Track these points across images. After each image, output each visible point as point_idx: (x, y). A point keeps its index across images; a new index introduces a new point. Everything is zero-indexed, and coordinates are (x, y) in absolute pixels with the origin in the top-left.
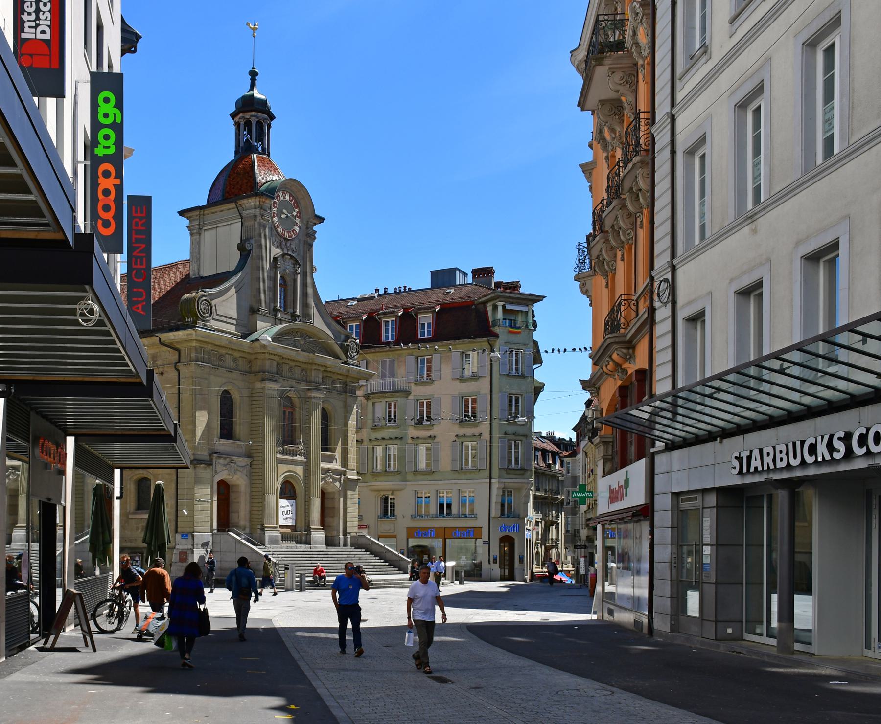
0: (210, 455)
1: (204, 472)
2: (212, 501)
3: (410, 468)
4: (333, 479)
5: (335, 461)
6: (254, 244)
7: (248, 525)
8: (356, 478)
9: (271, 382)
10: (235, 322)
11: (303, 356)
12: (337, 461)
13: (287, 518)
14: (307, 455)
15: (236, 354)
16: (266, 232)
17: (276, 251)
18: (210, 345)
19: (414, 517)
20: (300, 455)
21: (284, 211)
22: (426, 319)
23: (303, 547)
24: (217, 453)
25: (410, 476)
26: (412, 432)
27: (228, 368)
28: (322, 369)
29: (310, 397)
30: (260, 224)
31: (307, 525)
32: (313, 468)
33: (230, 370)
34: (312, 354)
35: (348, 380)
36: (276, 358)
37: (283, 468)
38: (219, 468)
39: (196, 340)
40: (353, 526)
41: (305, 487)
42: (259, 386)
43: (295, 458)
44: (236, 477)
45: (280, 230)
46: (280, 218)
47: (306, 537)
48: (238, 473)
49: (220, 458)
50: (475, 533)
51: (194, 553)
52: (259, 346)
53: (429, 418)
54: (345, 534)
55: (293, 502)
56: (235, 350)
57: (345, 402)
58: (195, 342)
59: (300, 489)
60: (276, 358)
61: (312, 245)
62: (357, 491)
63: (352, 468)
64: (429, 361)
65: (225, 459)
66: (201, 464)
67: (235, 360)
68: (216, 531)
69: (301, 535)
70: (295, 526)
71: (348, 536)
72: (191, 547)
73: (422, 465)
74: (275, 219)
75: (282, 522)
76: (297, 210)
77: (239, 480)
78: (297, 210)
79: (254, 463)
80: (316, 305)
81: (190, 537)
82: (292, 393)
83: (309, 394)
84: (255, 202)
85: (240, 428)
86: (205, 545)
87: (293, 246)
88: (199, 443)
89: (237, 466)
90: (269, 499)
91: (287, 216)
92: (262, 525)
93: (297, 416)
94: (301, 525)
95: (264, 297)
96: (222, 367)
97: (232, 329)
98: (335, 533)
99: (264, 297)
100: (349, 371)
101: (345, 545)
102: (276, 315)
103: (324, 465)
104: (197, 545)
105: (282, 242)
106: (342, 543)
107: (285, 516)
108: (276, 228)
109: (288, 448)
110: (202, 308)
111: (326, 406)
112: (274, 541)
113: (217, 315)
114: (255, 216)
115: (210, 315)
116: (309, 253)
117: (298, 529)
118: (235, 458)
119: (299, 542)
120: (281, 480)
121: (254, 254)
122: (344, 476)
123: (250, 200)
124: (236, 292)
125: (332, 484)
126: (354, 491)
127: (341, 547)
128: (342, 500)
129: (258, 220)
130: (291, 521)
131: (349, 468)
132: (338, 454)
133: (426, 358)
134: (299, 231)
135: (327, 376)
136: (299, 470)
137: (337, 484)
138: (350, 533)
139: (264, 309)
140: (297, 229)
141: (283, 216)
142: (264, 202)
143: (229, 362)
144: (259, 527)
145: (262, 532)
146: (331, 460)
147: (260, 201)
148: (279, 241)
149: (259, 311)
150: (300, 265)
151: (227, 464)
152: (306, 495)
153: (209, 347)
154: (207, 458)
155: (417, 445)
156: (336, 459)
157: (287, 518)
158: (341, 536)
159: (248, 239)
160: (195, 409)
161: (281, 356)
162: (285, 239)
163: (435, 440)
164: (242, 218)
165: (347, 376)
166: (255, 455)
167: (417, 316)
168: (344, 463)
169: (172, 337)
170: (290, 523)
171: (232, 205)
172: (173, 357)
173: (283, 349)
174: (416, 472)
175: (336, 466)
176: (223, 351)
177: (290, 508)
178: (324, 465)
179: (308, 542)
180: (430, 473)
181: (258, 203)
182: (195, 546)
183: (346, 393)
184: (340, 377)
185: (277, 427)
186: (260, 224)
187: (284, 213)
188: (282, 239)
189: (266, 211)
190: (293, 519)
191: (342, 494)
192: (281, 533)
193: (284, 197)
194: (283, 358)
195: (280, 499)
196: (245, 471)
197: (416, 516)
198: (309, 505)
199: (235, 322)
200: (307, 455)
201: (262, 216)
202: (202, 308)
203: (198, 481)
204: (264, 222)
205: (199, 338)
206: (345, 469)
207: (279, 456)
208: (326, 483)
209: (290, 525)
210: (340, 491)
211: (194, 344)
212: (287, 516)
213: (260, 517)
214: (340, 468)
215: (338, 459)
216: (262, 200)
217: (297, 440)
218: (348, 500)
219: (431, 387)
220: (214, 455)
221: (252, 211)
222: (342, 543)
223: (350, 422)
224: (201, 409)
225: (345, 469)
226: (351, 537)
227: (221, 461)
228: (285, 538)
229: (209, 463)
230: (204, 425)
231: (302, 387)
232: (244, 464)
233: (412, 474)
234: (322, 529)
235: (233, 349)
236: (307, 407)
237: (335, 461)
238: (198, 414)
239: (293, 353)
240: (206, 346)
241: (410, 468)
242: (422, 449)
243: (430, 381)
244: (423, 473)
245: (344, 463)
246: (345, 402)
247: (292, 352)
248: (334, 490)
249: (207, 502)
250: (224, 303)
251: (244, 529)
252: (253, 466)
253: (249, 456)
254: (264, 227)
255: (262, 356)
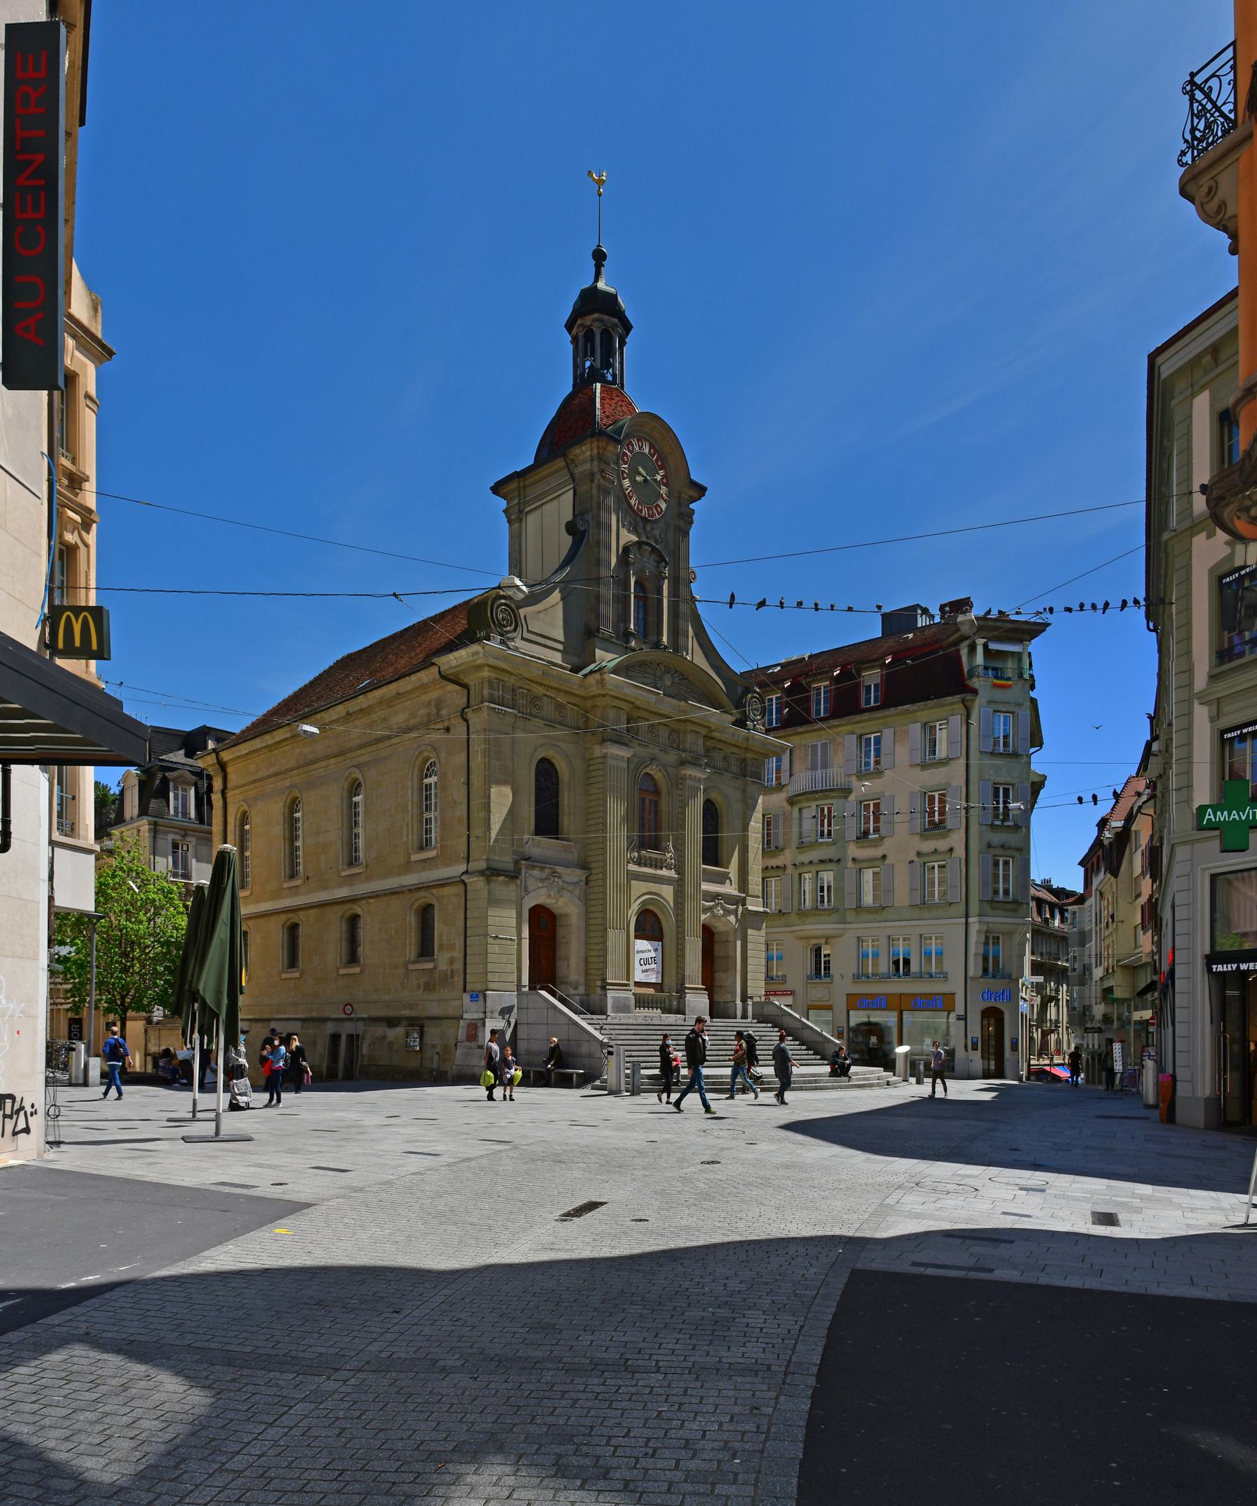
0: (517, 863)
1: (501, 887)
2: (520, 939)
3: (850, 902)
4: (724, 909)
5: (728, 881)
6: (590, 521)
7: (582, 980)
8: (761, 909)
9: (617, 745)
10: (560, 647)
11: (669, 706)
12: (731, 881)
13: (647, 971)
14: (680, 869)
15: (561, 699)
16: (611, 501)
17: (628, 537)
18: (513, 677)
19: (857, 977)
20: (667, 868)
21: (640, 469)
22: (872, 677)
23: (672, 1018)
24: (527, 859)
25: (850, 916)
26: (853, 851)
27: (547, 720)
28: (703, 731)
29: (684, 778)
30: (599, 486)
31: (680, 982)
32: (688, 889)
33: (551, 724)
34: (683, 703)
35: (749, 756)
36: (625, 706)
37: (638, 887)
38: (531, 884)
39: (489, 666)
40: (757, 988)
41: (677, 921)
42: (598, 751)
43: (659, 872)
44: (562, 901)
45: (633, 502)
46: (633, 482)
47: (679, 1003)
48: (565, 892)
49: (533, 867)
50: (944, 1003)
51: (487, 1024)
52: (595, 682)
53: (876, 830)
54: (744, 998)
55: (658, 944)
56: (558, 690)
57: (744, 791)
58: (486, 668)
59: (669, 924)
60: (625, 706)
61: (687, 534)
62: (763, 932)
63: (756, 894)
64: (878, 741)
65: (542, 869)
66: (499, 875)
67: (559, 706)
68: (527, 989)
69: (670, 997)
70: (661, 984)
71: (750, 1002)
72: (481, 1015)
73: (868, 899)
74: (626, 483)
75: (639, 976)
76: (662, 472)
77: (567, 906)
78: (662, 472)
79: (592, 878)
80: (696, 634)
81: (481, 996)
82: (654, 767)
83: (683, 772)
84: (592, 450)
85: (568, 821)
86: (505, 1012)
87: (657, 533)
88: (496, 840)
89: (563, 881)
90: (615, 938)
91: (645, 481)
92: (604, 980)
93: (664, 806)
94: (671, 982)
95: (609, 611)
96: (536, 717)
97: (557, 658)
98: (728, 998)
99: (609, 611)
100: (747, 740)
101: (744, 1016)
102: (628, 642)
103: (706, 887)
104: (492, 1012)
105: (637, 522)
106: (739, 1013)
107: (645, 967)
108: (626, 499)
109: (648, 855)
110: (500, 617)
111: (714, 796)
112: (622, 1007)
113: (529, 631)
114: (592, 475)
115: (515, 630)
116: (682, 546)
117: (666, 989)
118: (559, 869)
119: (667, 1010)
120: (635, 907)
121: (591, 539)
122: (743, 905)
123: (583, 448)
124: (563, 599)
125: (723, 918)
126: (759, 929)
127: (738, 1020)
128: (739, 943)
129: (596, 481)
130: (655, 976)
131: (750, 893)
132: (733, 870)
133: (872, 736)
134: (667, 508)
135: (714, 748)
136: (667, 892)
137: (732, 918)
138: (751, 998)
139: (607, 630)
140: (663, 506)
141: (639, 479)
142: (605, 449)
143: (549, 710)
144: (599, 983)
145: (603, 993)
146: (722, 879)
147: (598, 448)
148: (633, 522)
149: (599, 632)
150: (667, 564)
151: (546, 879)
152: (678, 933)
153: (512, 681)
154: (511, 867)
155: (860, 869)
156: (730, 878)
157: (647, 971)
158: (739, 1002)
159: (582, 514)
160: (489, 782)
161: (633, 703)
162: (644, 519)
163: (887, 862)
164: (574, 480)
165: (746, 749)
166: (594, 865)
167: (859, 675)
168: (743, 884)
169: (454, 663)
170: (653, 979)
171: (560, 463)
172: (454, 696)
173: (634, 690)
174: (859, 908)
175: (730, 889)
176: (540, 690)
177: (653, 954)
178: (706, 887)
179: (681, 1011)
180: (879, 910)
181: (595, 451)
182: (488, 1014)
183: (745, 776)
184: (736, 750)
185: (628, 818)
186: (599, 486)
187: (640, 474)
188: (638, 519)
189: (609, 465)
190: (657, 972)
191: (739, 934)
192: (634, 994)
193: (640, 448)
194: (638, 708)
195: (637, 937)
196: (577, 892)
197: (859, 977)
198: (683, 950)
199: (560, 647)
200: (680, 869)
201: (602, 471)
202: (500, 617)
203: (493, 901)
204: (606, 484)
205: (492, 661)
206: (743, 895)
207: (632, 867)
208: (714, 916)
209: (654, 981)
210: (736, 930)
211: (486, 673)
212: (648, 967)
213: (601, 967)
214: (736, 893)
215: (732, 879)
216: (600, 444)
217: (663, 844)
218: (750, 946)
219: (880, 780)
220: (522, 862)
221: (587, 466)
222: (739, 1013)
223: (752, 823)
224: (499, 782)
225: (743, 895)
226: (754, 1004)
227: (536, 873)
228: (641, 1002)
229: (513, 875)
230: (505, 811)
231: (672, 757)
232: (574, 880)
233: (854, 913)
234: (705, 990)
235: (555, 689)
236: (680, 792)
237: (728, 881)
238: (494, 790)
239: (653, 699)
240: (506, 679)
241: (850, 902)
242: (868, 875)
243: (879, 773)
244: (869, 910)
245: (743, 884)
246: (744, 791)
247: (650, 695)
248: (727, 929)
249: (511, 939)
250: (541, 615)
251: (576, 988)
252: (591, 884)
253: (584, 866)
254: (607, 492)
255: (600, 702)
